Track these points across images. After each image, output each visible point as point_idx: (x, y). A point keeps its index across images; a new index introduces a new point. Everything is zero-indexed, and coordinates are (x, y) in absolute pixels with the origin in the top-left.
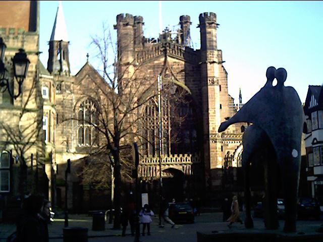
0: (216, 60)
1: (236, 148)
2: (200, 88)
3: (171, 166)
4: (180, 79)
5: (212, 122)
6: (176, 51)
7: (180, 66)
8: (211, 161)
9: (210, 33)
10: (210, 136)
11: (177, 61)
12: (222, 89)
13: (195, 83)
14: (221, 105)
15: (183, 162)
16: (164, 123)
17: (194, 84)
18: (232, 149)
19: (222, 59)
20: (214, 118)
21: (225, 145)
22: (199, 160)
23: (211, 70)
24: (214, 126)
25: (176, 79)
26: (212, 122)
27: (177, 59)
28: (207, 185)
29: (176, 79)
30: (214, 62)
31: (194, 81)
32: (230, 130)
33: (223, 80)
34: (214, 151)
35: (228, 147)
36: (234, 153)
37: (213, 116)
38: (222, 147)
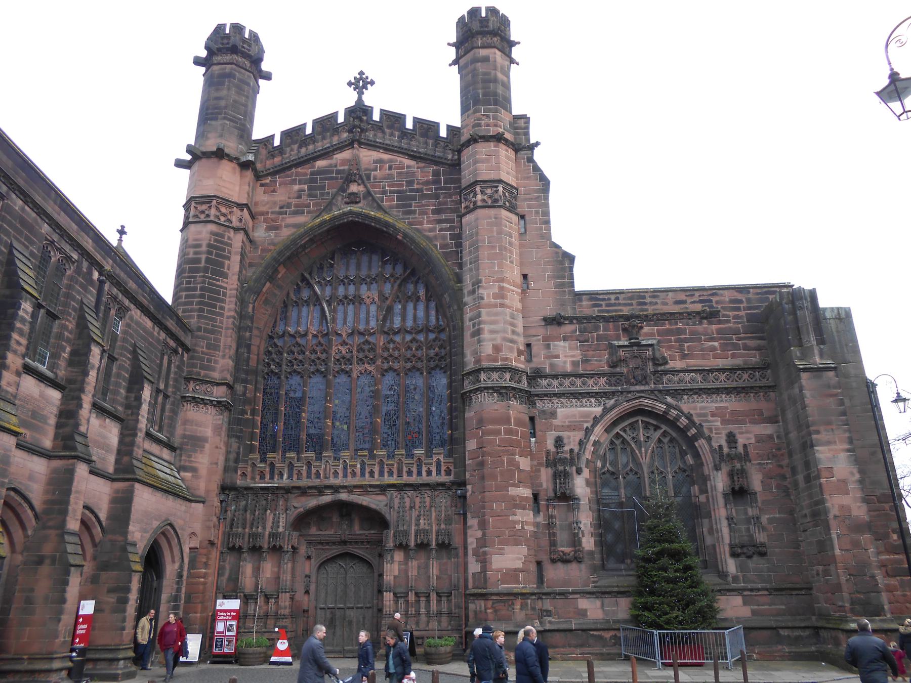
0: (508, 136)
1: (589, 425)
2: (457, 231)
3: (344, 496)
4: (391, 207)
5: (492, 327)
6: (388, 131)
7: (394, 172)
8: (487, 471)
9: (486, 59)
10: (483, 376)
11: (386, 157)
12: (528, 226)
13: (443, 217)
14: (525, 277)
15: (387, 480)
16: (339, 351)
17: (440, 221)
18: (571, 427)
19: (528, 140)
20: (496, 314)
21: (543, 412)
22: (448, 472)
23: (487, 161)
24: (499, 341)
25: (380, 208)
26: (492, 327)
27: (387, 149)
28: (474, 567)
29: (380, 208)
30: (499, 138)
31: (437, 212)
32: (562, 359)
33: (530, 199)
34: (498, 432)
35: (555, 422)
36: (581, 443)
37: (495, 306)
38: (532, 419)
